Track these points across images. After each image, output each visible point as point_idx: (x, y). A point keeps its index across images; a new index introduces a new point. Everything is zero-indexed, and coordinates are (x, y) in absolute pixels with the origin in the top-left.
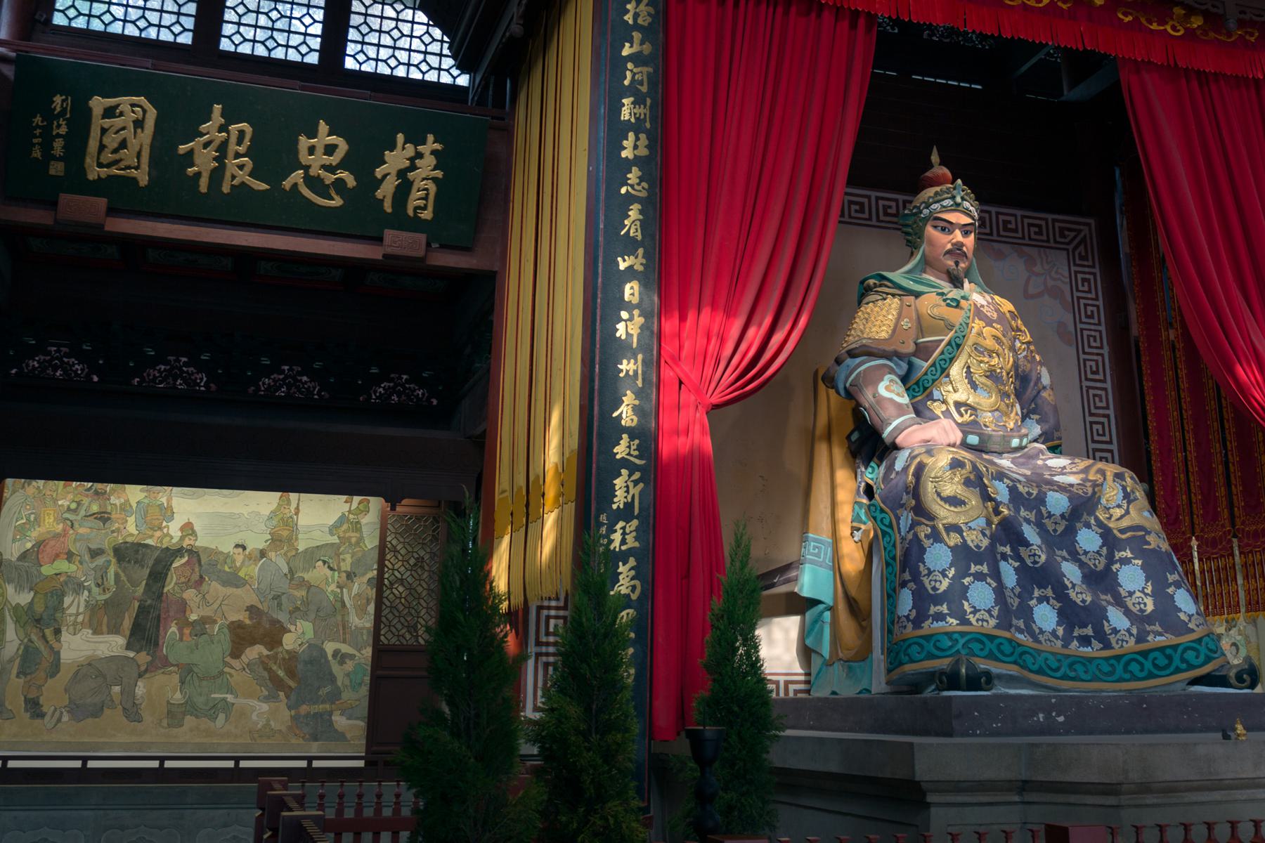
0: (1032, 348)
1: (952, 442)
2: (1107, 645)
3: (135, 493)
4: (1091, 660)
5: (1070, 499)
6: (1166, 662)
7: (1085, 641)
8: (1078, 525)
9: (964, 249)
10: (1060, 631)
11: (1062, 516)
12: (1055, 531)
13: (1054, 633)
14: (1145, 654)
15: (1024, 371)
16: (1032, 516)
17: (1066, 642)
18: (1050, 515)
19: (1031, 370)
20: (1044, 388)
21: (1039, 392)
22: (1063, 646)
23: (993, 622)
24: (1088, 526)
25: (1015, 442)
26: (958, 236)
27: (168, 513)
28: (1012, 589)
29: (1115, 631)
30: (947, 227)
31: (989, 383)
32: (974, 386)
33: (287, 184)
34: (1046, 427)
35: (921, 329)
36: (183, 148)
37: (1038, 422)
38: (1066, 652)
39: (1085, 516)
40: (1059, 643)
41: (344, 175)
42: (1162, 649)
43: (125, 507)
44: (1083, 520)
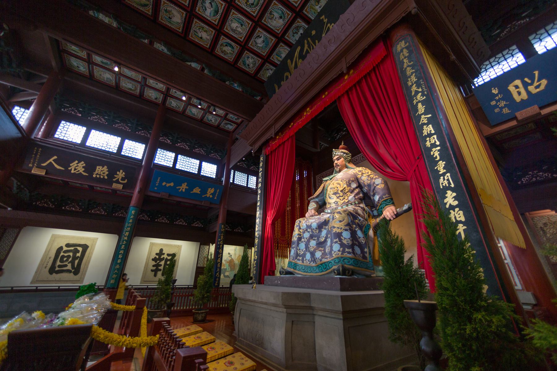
0: (370, 176)
1: (311, 214)
2: (316, 263)
4: (312, 267)
6: (325, 267)
7: (314, 263)
8: (322, 230)
9: (338, 164)
10: (310, 260)
11: (316, 228)
12: (316, 232)
13: (309, 261)
14: (322, 264)
15: (367, 184)
17: (311, 262)
18: (314, 229)
19: (370, 182)
20: (377, 185)
21: (375, 187)
22: (309, 264)
23: (292, 258)
24: (325, 229)
28: (302, 250)
29: (316, 258)
31: (333, 195)
32: (330, 198)
34: (380, 196)
37: (378, 195)
38: (309, 265)
39: (324, 227)
40: (309, 263)
42: (325, 263)
44: (324, 228)
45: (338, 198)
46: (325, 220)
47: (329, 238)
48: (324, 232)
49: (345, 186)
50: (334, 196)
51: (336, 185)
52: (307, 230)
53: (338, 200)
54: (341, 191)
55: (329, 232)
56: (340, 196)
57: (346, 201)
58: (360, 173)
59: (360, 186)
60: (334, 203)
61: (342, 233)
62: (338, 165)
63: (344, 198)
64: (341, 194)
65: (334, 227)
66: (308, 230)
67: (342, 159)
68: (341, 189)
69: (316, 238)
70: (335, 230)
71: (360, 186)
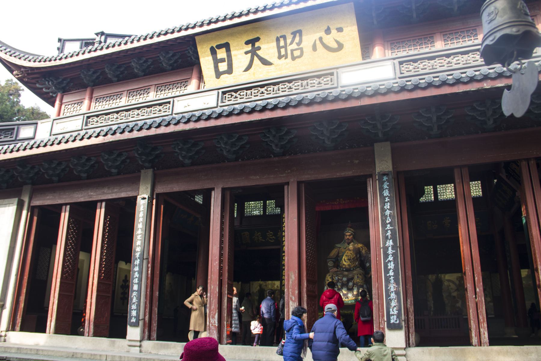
2: (348, 299)
3: (270, 282)
5: (347, 279)
7: (346, 298)
16: (341, 281)
24: (351, 282)
25: (352, 269)
26: (348, 237)
27: (274, 284)
30: (347, 236)
32: (345, 261)
33: (267, 240)
35: (338, 253)
36: (253, 237)
41: (273, 237)
43: (269, 284)
45: (351, 262)
46: (352, 277)
47: (355, 287)
48: (351, 284)
49: (355, 255)
50: (348, 261)
51: (349, 254)
52: (338, 281)
53: (351, 264)
54: (353, 259)
55: (354, 284)
56: (352, 262)
57: (355, 265)
58: (361, 248)
59: (360, 256)
60: (348, 265)
61: (363, 285)
62: (349, 240)
63: (354, 263)
64: (353, 261)
65: (359, 282)
66: (340, 281)
67: (352, 236)
68: (353, 257)
69: (346, 286)
70: (359, 284)
71: (360, 256)
